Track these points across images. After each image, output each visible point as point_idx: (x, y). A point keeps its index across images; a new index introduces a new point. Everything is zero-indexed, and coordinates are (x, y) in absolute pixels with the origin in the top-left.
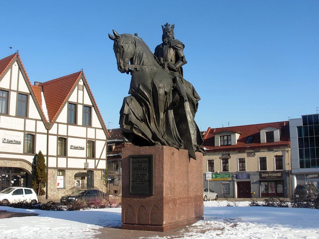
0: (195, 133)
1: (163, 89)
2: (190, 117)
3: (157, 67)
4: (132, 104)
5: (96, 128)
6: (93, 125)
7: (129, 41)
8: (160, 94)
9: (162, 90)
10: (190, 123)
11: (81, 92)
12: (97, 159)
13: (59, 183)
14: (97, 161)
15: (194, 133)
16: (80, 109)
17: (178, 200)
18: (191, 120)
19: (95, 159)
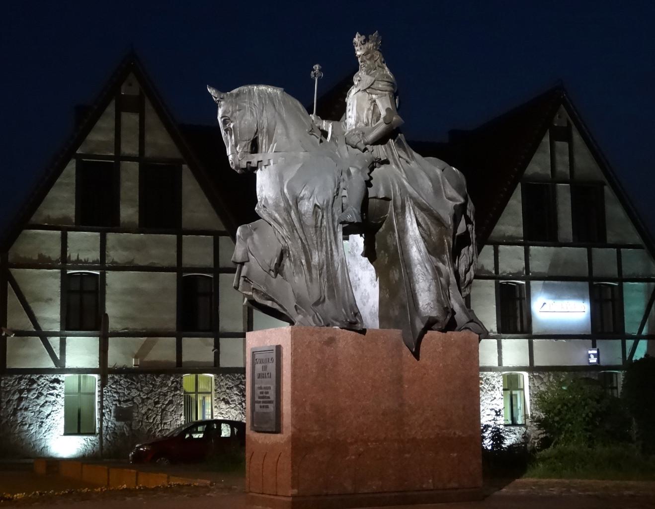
0: (431, 286)
1: (311, 200)
2: (420, 251)
3: (306, 151)
4: (252, 239)
5: (618, 246)
6: (611, 238)
7: (245, 104)
8: (303, 213)
9: (307, 203)
10: (419, 264)
11: (562, 146)
12: (631, 337)
13: (269, 406)
14: (630, 343)
15: (429, 288)
16: (564, 193)
17: (351, 444)
18: (421, 257)
19: (624, 337)
